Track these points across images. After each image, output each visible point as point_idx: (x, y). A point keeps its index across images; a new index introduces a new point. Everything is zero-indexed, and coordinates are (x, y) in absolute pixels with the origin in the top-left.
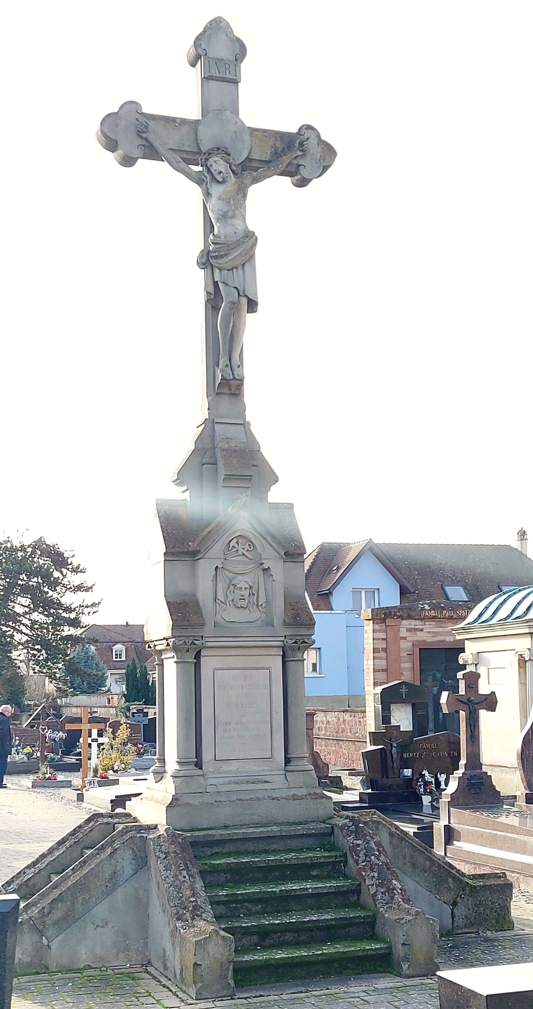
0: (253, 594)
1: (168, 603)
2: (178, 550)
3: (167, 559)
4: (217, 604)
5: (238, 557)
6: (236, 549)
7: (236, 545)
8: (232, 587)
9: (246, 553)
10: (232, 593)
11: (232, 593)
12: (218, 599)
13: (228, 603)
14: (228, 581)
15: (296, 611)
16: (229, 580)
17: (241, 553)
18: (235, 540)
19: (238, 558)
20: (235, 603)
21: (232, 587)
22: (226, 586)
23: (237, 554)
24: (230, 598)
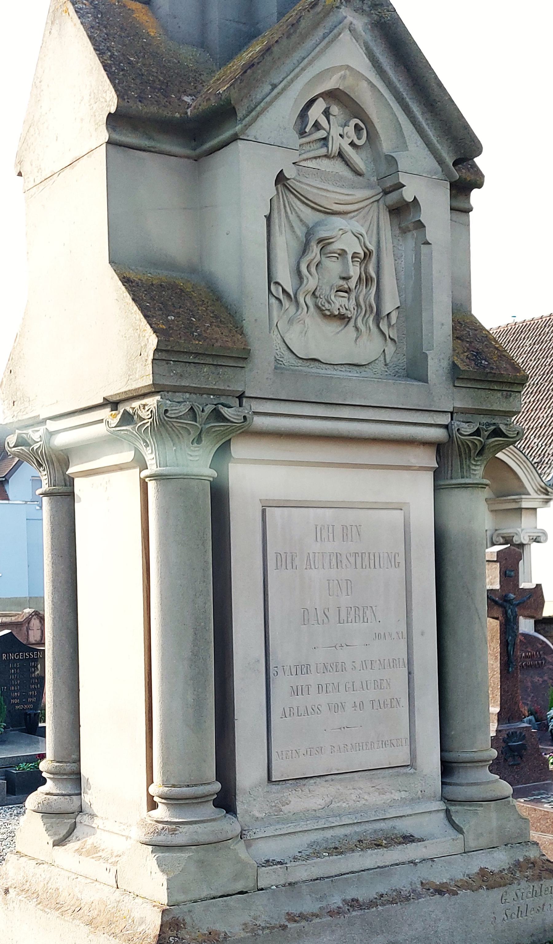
0: (369, 280)
1: (126, 281)
2: (154, 109)
3: (117, 137)
4: (273, 300)
5: (325, 161)
6: (322, 134)
7: (323, 121)
8: (315, 249)
9: (349, 151)
10: (313, 269)
11: (313, 269)
12: (277, 283)
13: (301, 300)
14: (300, 231)
15: (471, 342)
16: (304, 230)
17: (335, 150)
18: (320, 105)
19: (325, 165)
20: (320, 302)
21: (315, 249)
22: (295, 246)
23: (323, 151)
24: (311, 283)
